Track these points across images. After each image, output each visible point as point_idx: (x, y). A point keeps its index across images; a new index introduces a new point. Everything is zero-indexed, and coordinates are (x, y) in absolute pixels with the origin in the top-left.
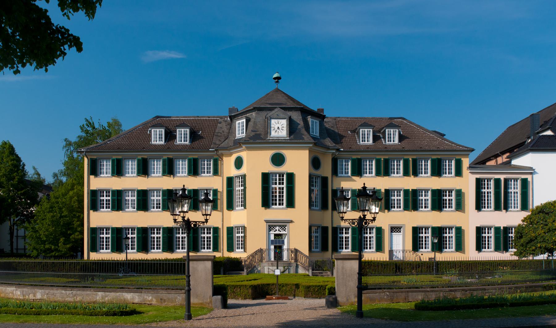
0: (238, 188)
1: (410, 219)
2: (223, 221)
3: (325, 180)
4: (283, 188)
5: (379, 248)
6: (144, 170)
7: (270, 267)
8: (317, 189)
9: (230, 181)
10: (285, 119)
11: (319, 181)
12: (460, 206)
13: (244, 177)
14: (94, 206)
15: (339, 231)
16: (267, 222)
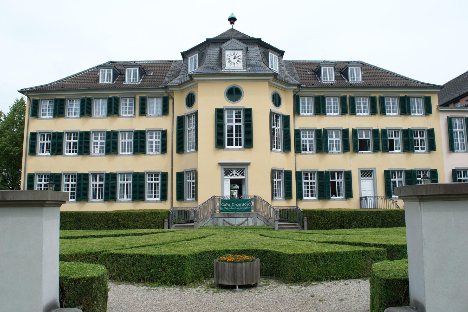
0: (189, 127)
1: (381, 162)
2: (172, 166)
3: (286, 119)
4: (240, 126)
5: (349, 195)
6: (86, 110)
7: (226, 219)
8: (279, 128)
9: (181, 121)
10: (242, 49)
11: (280, 120)
12: (432, 147)
13: (196, 114)
14: (33, 152)
15: (303, 176)
16: (221, 164)
